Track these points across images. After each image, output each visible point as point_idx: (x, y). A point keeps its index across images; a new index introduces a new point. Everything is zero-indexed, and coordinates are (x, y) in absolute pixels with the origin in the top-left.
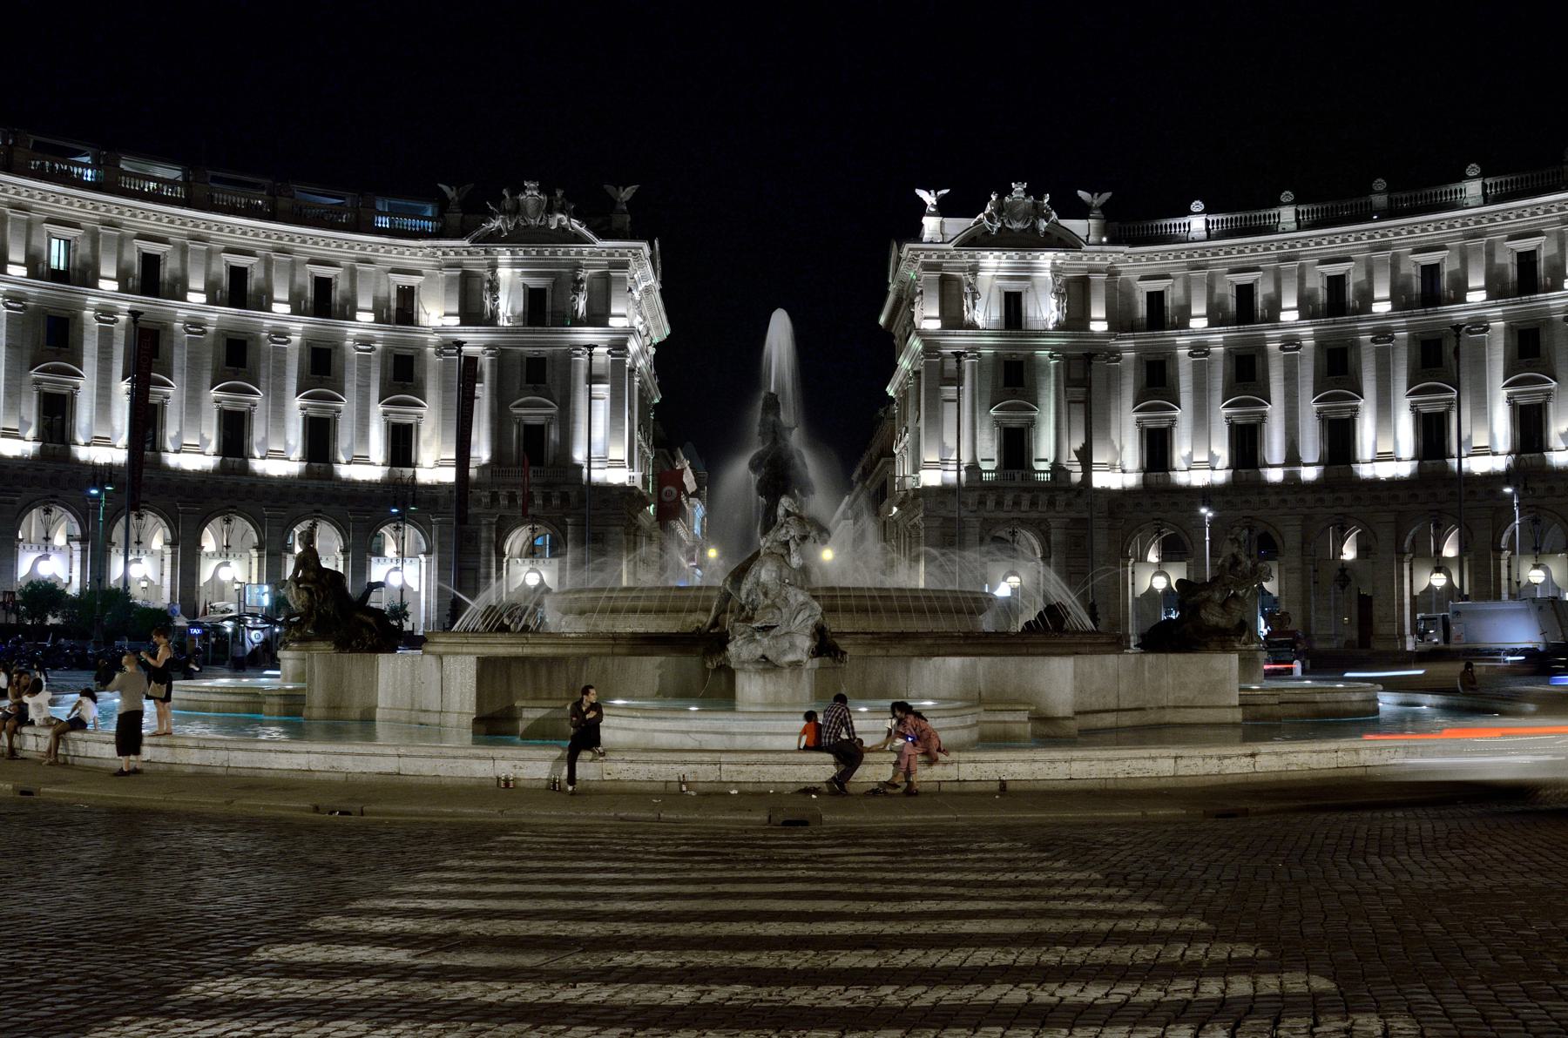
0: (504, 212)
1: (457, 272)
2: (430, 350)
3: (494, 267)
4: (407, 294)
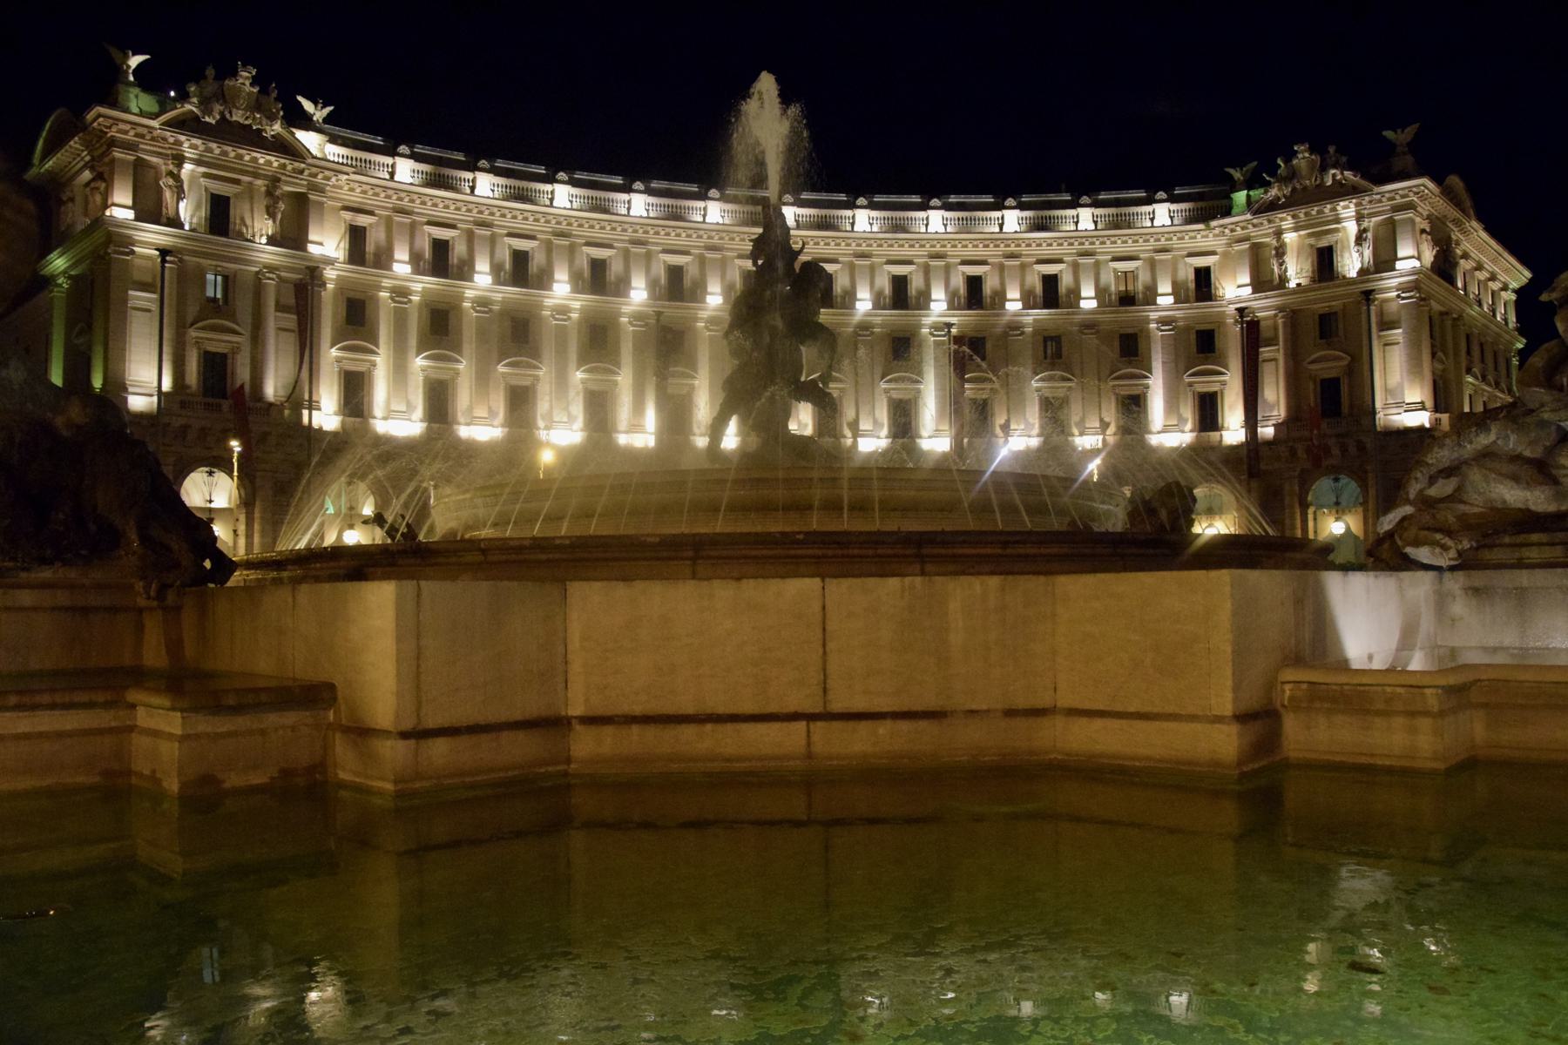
1: (1246, 246)
3: (1279, 233)
4: (1203, 275)
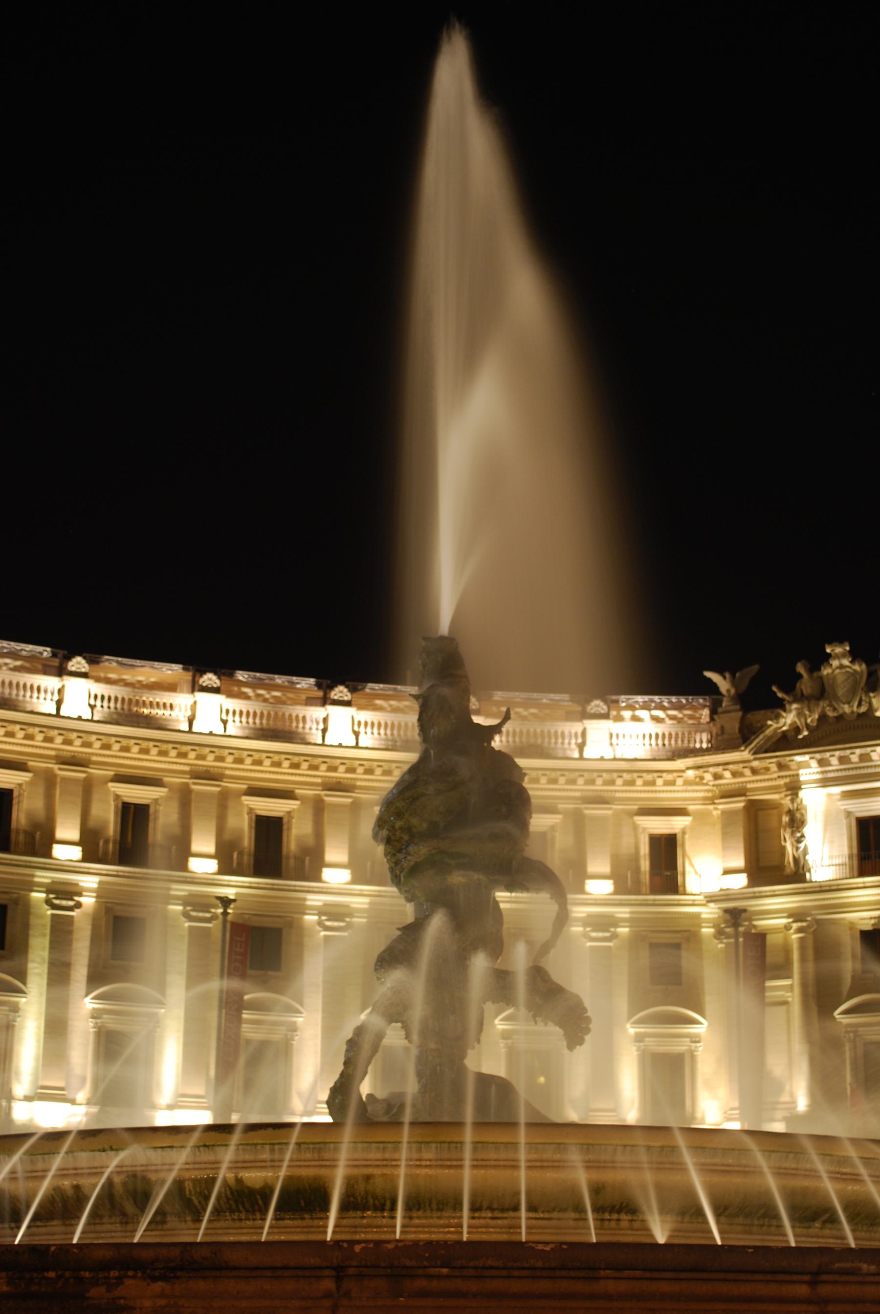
0: (800, 698)
1: (739, 804)
2: (707, 931)
3: (794, 788)
4: (666, 850)
